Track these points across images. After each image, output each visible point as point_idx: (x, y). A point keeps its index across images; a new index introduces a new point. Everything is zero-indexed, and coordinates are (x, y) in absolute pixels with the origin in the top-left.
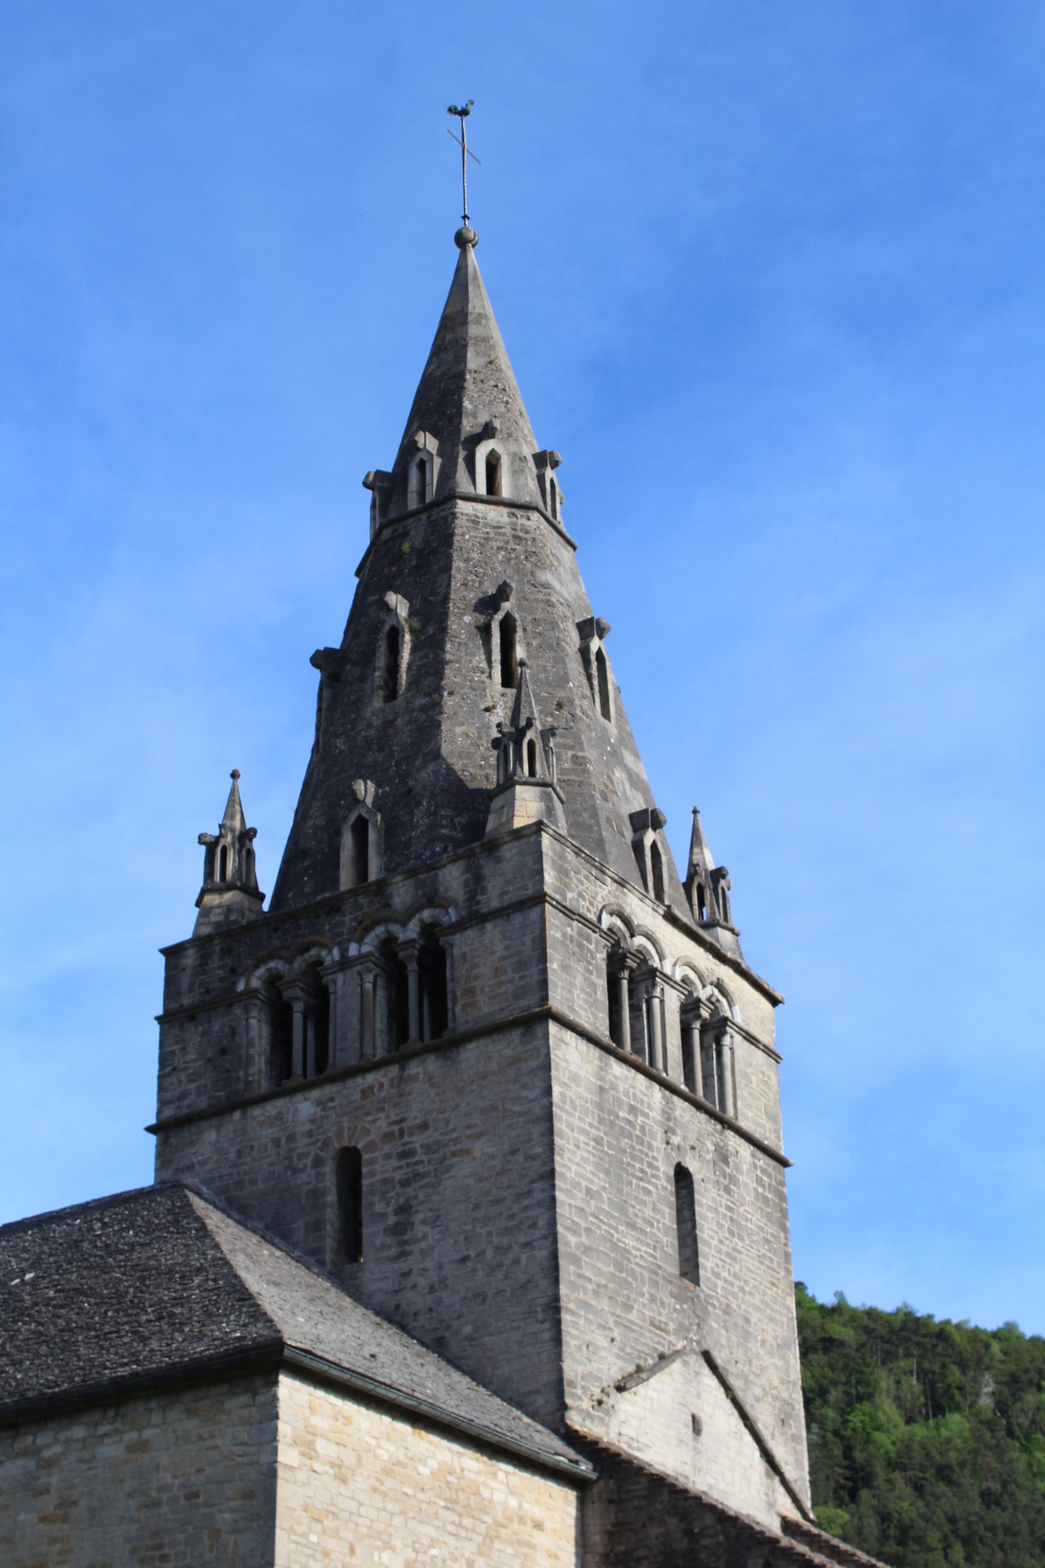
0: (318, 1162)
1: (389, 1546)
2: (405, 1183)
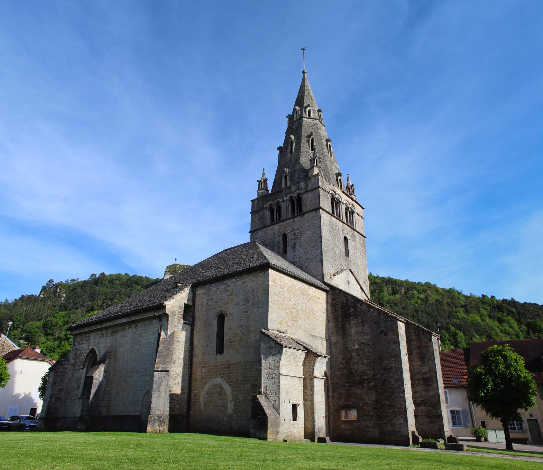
0: (279, 236)
1: (290, 300)
2: (295, 239)
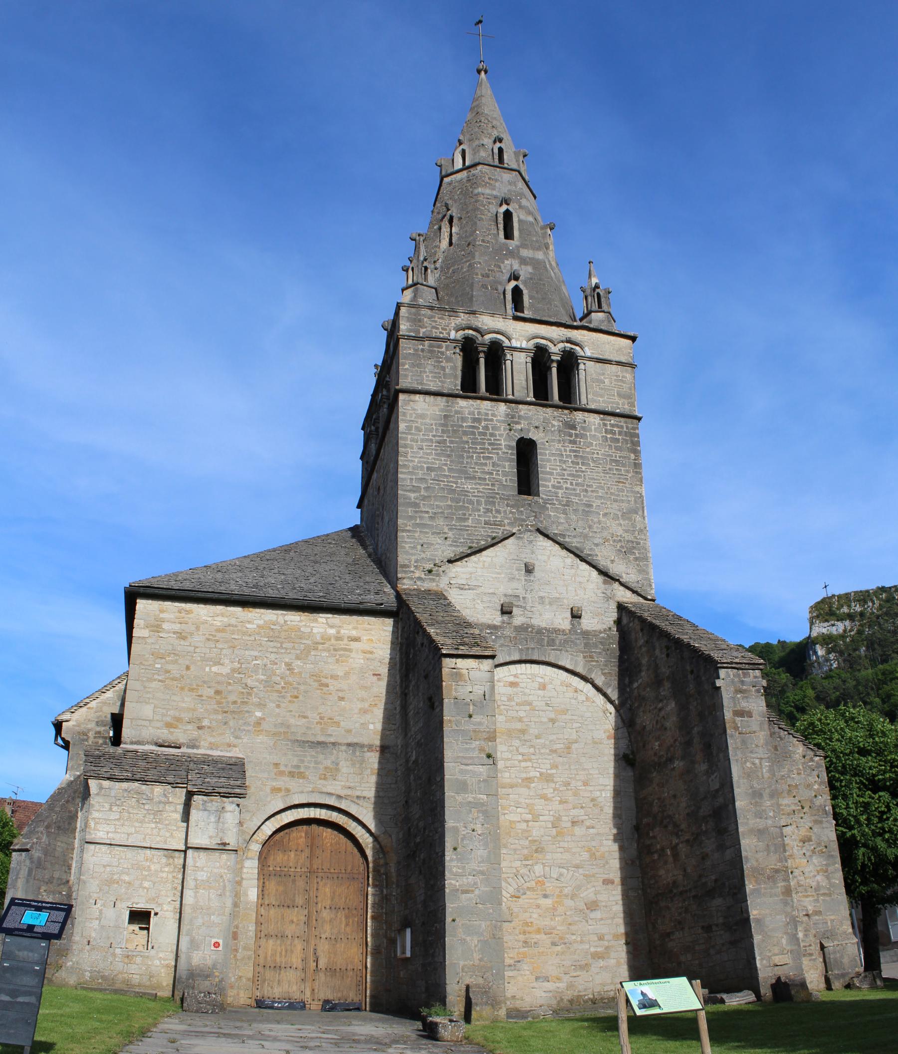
1: (218, 663)
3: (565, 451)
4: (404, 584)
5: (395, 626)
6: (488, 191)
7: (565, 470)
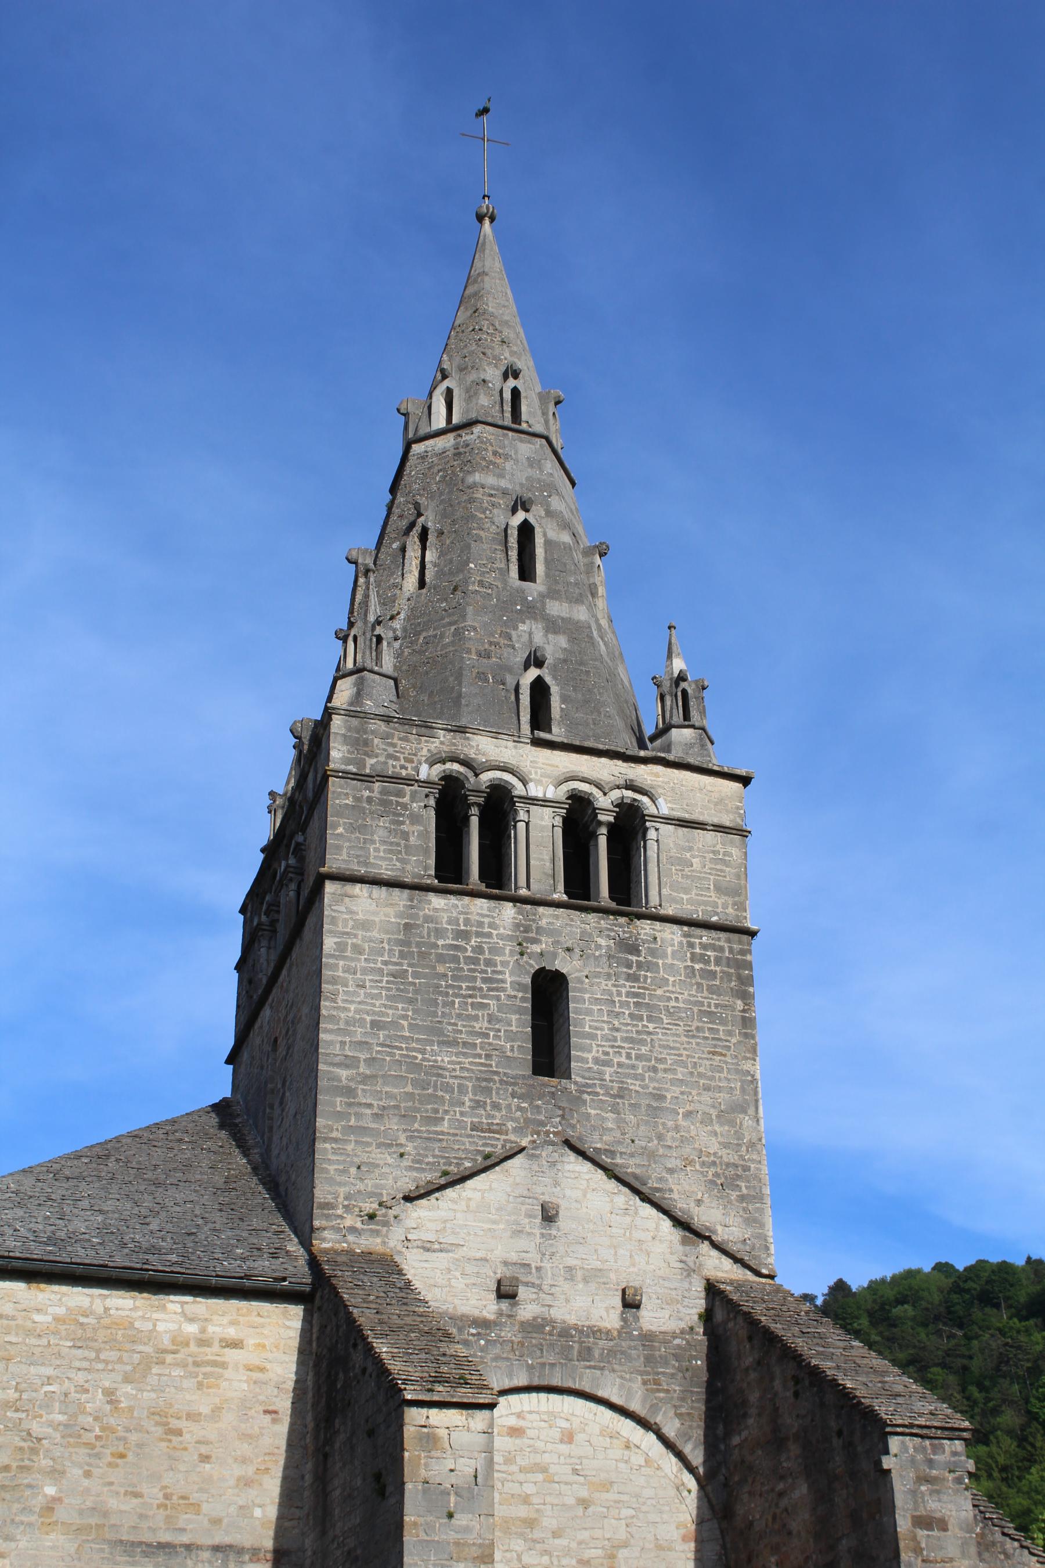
3: (619, 994)
4: (324, 1240)
5: (307, 1320)
6: (490, 480)
7: (617, 1030)
